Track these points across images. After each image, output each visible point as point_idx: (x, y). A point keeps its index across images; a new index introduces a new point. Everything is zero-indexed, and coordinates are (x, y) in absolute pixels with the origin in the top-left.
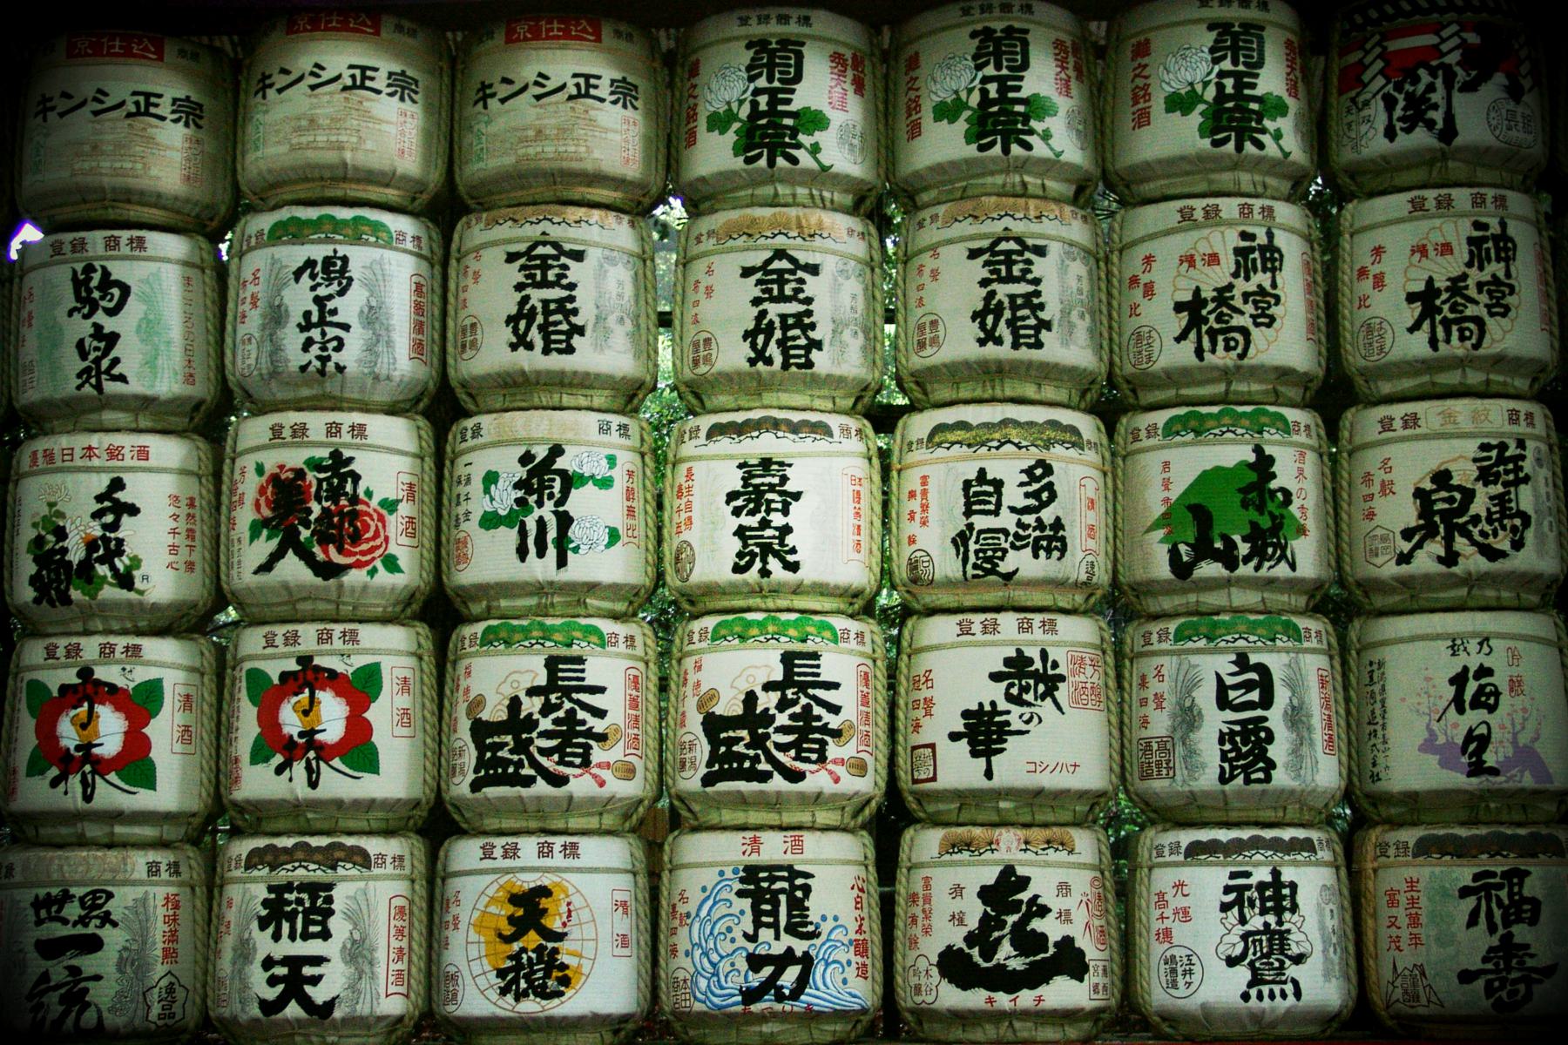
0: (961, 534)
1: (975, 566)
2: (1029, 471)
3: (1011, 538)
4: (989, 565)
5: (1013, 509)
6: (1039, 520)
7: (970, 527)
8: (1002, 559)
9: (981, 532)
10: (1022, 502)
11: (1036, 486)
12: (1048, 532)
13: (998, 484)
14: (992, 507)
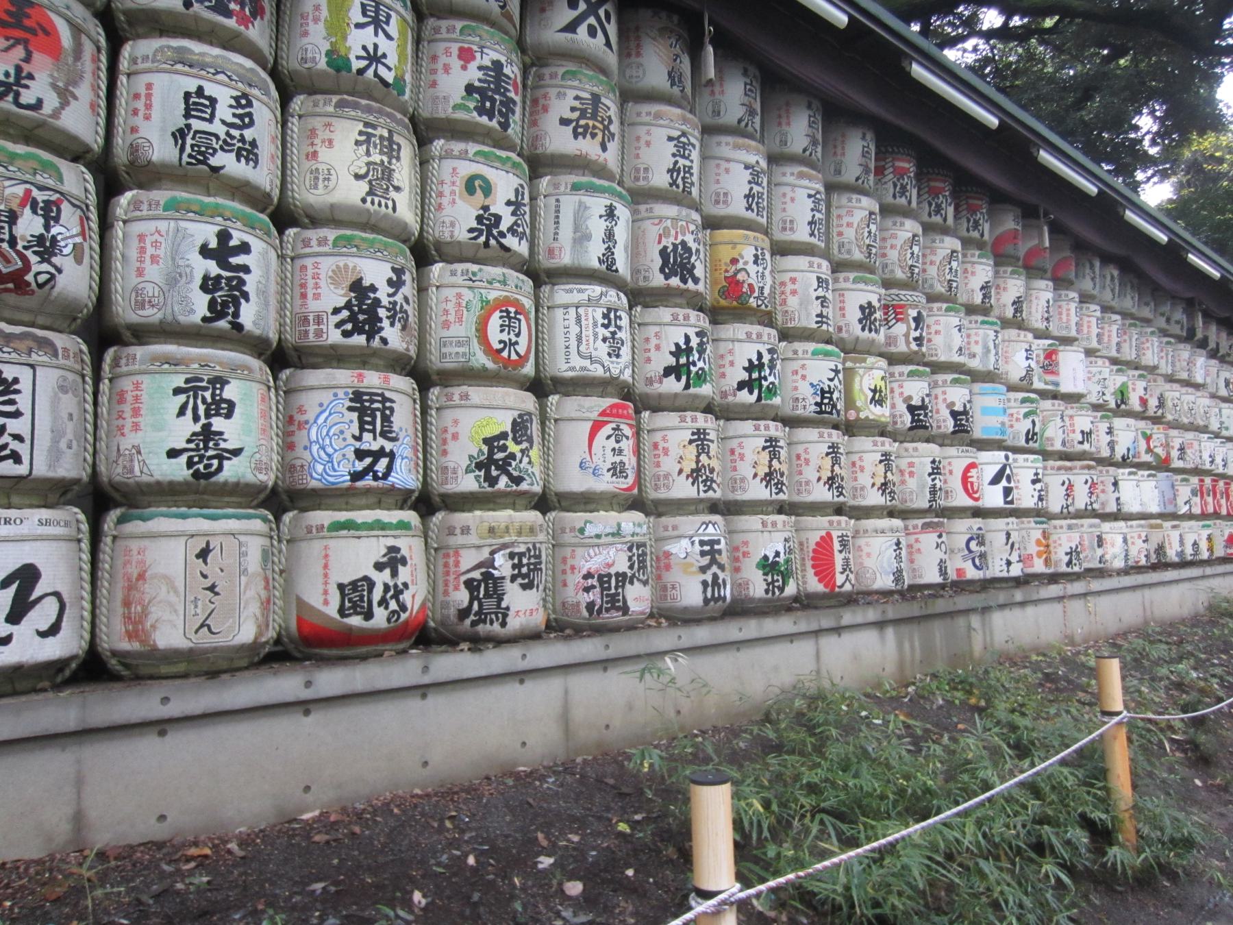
0: (181, 131)
1: (190, 156)
2: (237, 99)
3: (220, 142)
4: (201, 157)
5: (223, 122)
6: (242, 135)
7: (189, 127)
8: (212, 155)
9: (196, 132)
10: (231, 119)
11: (240, 111)
12: (247, 146)
13: (213, 101)
14: (207, 116)
